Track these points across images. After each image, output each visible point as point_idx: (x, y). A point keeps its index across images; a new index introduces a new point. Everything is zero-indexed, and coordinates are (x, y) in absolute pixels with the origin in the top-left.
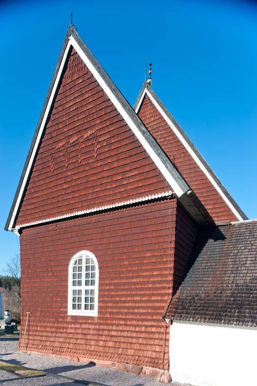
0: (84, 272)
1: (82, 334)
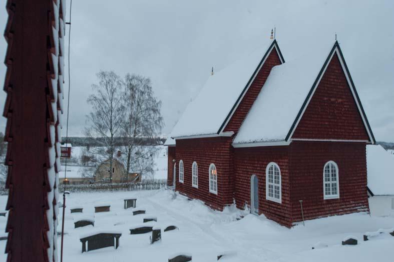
1: (333, 210)
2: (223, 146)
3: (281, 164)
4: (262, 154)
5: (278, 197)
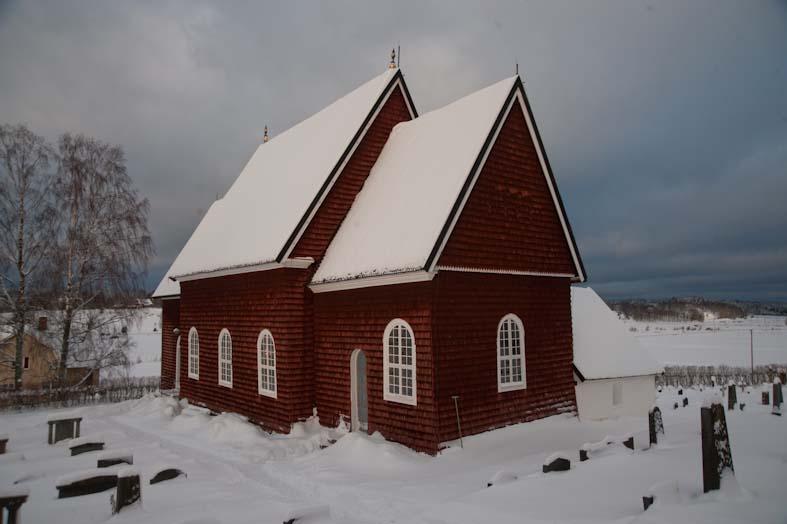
2: (290, 290)
3: (416, 321)
4: (372, 304)
5: (410, 394)
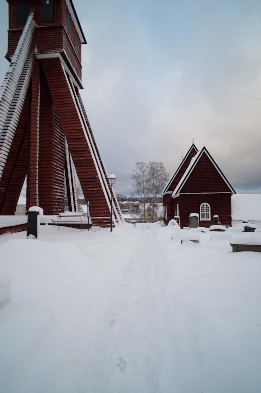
0: (205, 209)
